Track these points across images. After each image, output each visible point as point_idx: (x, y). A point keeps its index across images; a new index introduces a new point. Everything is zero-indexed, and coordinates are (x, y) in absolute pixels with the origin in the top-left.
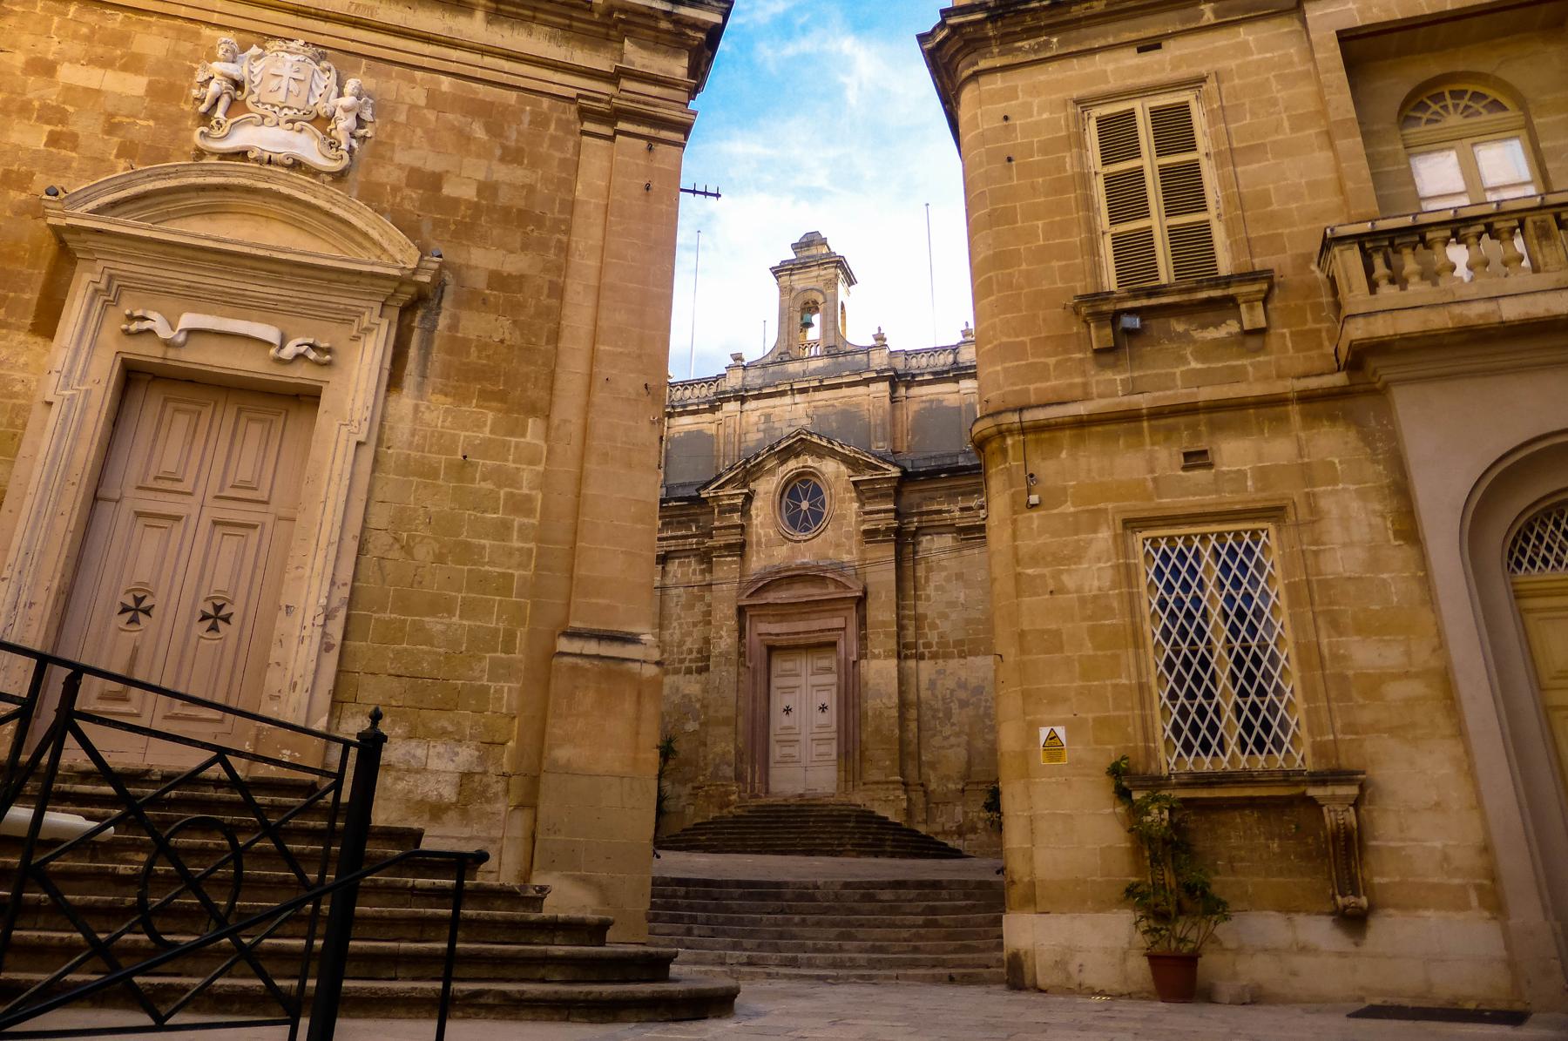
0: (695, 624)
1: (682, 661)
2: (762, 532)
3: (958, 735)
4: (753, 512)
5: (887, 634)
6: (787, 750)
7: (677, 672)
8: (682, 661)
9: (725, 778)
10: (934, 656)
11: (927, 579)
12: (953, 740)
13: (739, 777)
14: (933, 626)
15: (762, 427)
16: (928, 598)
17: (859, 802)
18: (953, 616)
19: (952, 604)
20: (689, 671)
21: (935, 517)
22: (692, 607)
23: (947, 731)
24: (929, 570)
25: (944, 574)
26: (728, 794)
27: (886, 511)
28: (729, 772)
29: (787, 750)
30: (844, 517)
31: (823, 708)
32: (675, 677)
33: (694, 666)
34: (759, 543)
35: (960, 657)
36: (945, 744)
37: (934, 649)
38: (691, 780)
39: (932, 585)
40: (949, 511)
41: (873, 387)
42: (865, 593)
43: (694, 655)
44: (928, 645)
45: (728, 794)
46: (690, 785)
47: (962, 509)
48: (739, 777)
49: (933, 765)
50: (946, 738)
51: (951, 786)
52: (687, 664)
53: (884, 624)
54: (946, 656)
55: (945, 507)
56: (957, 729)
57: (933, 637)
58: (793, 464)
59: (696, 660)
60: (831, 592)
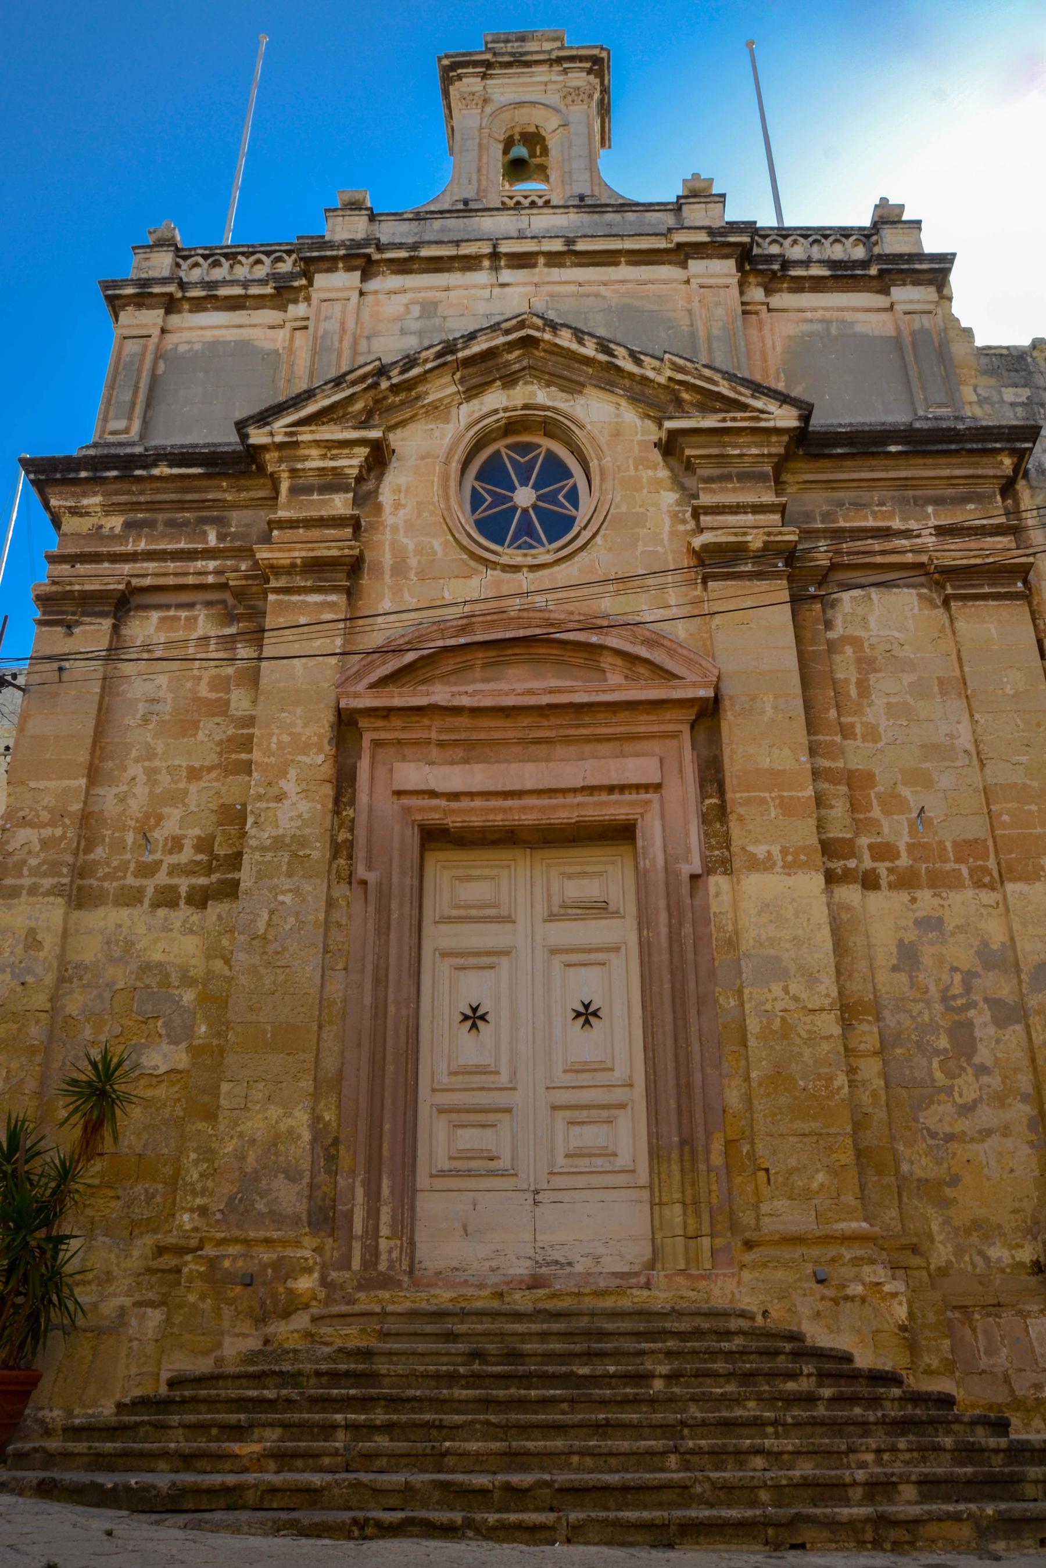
0: (194, 774)
1: (148, 870)
2: (409, 544)
3: (1000, 1100)
4: (386, 497)
5: (787, 808)
6: (469, 1139)
7: (130, 898)
8: (148, 870)
9: (277, 1219)
10: (906, 881)
11: (864, 687)
12: (987, 1116)
13: (325, 1217)
14: (893, 803)
15: (415, 325)
16: (872, 734)
17: (748, 1302)
18: (945, 781)
19: (935, 751)
20: (167, 899)
21: (877, 545)
22: (187, 727)
23: (968, 1088)
24: (866, 664)
25: (908, 678)
26: (284, 1270)
27: (757, 509)
28: (289, 1197)
29: (469, 1139)
30: (640, 520)
31: (587, 1014)
32: (124, 914)
33: (184, 884)
34: (400, 569)
35: (978, 884)
36: (963, 1125)
37: (904, 861)
38: (151, 1226)
39: (879, 702)
40: (906, 534)
41: (696, 266)
42: (717, 700)
43: (188, 854)
44: (884, 852)
45: (284, 1270)
46: (149, 1240)
47: (941, 531)
48: (325, 1217)
49: (936, 1191)
50: (966, 1110)
51: (998, 1252)
52: (162, 878)
53: (776, 778)
54: (939, 882)
55: (897, 524)
56: (994, 1081)
57: (895, 829)
58: (496, 400)
59: (189, 870)
60: (616, 685)
